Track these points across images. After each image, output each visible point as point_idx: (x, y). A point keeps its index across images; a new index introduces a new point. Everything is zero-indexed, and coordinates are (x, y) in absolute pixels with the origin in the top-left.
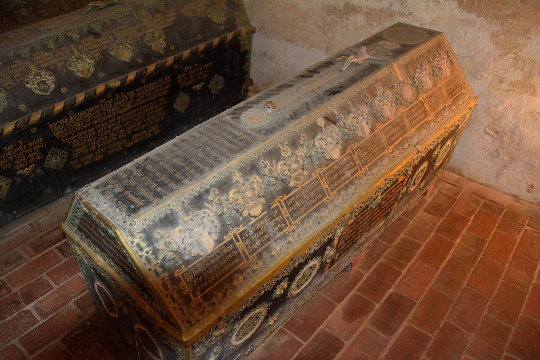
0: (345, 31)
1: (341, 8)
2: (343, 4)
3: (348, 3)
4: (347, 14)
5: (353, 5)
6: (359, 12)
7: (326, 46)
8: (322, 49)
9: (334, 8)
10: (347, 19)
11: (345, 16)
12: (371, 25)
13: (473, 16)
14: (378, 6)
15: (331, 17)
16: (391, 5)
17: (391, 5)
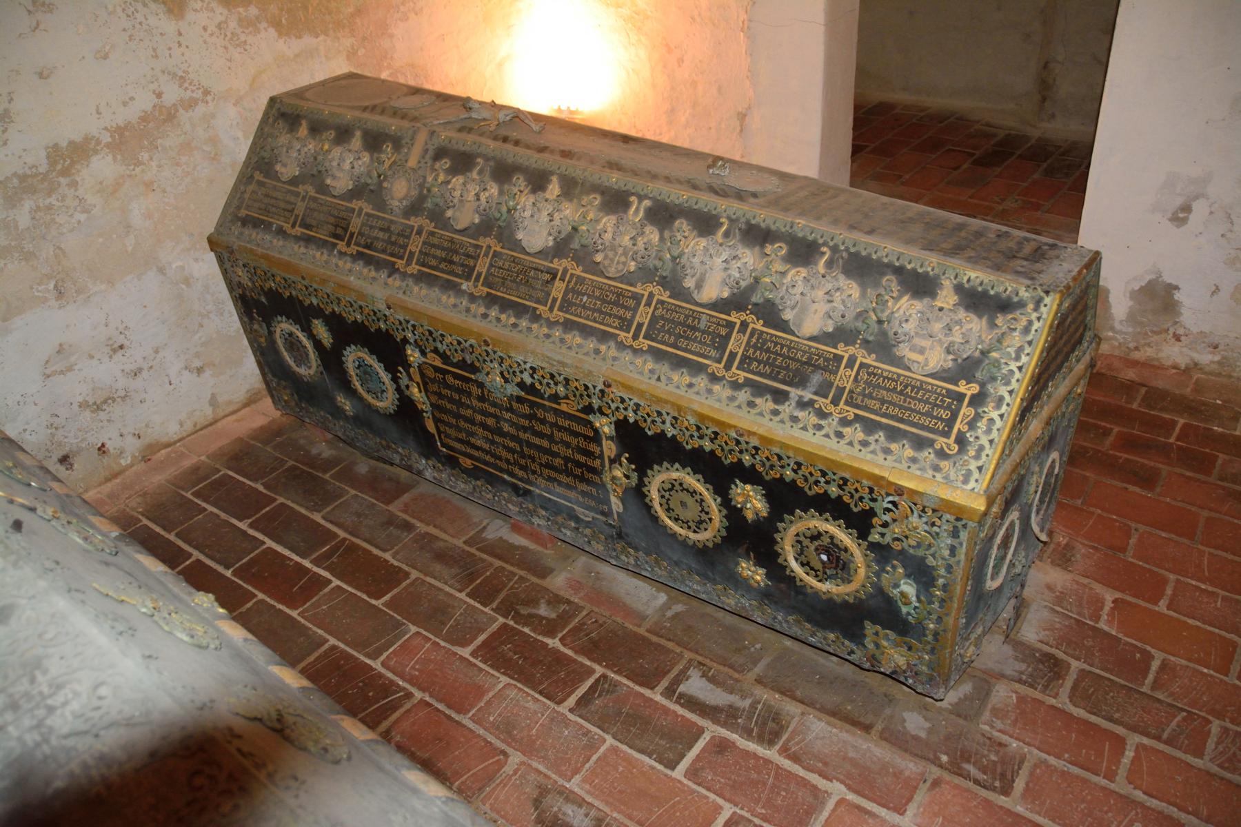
0: (82, 217)
1: (41, 170)
2: (43, 154)
3: (56, 145)
4: (65, 172)
5: (71, 143)
6: (96, 152)
7: (51, 286)
8: (46, 300)
9: (23, 178)
10: (74, 184)
11: (63, 181)
12: (139, 163)
13: (308, 41)
14: (131, 114)
15: (28, 204)
16: (159, 95)
17: (159, 95)
